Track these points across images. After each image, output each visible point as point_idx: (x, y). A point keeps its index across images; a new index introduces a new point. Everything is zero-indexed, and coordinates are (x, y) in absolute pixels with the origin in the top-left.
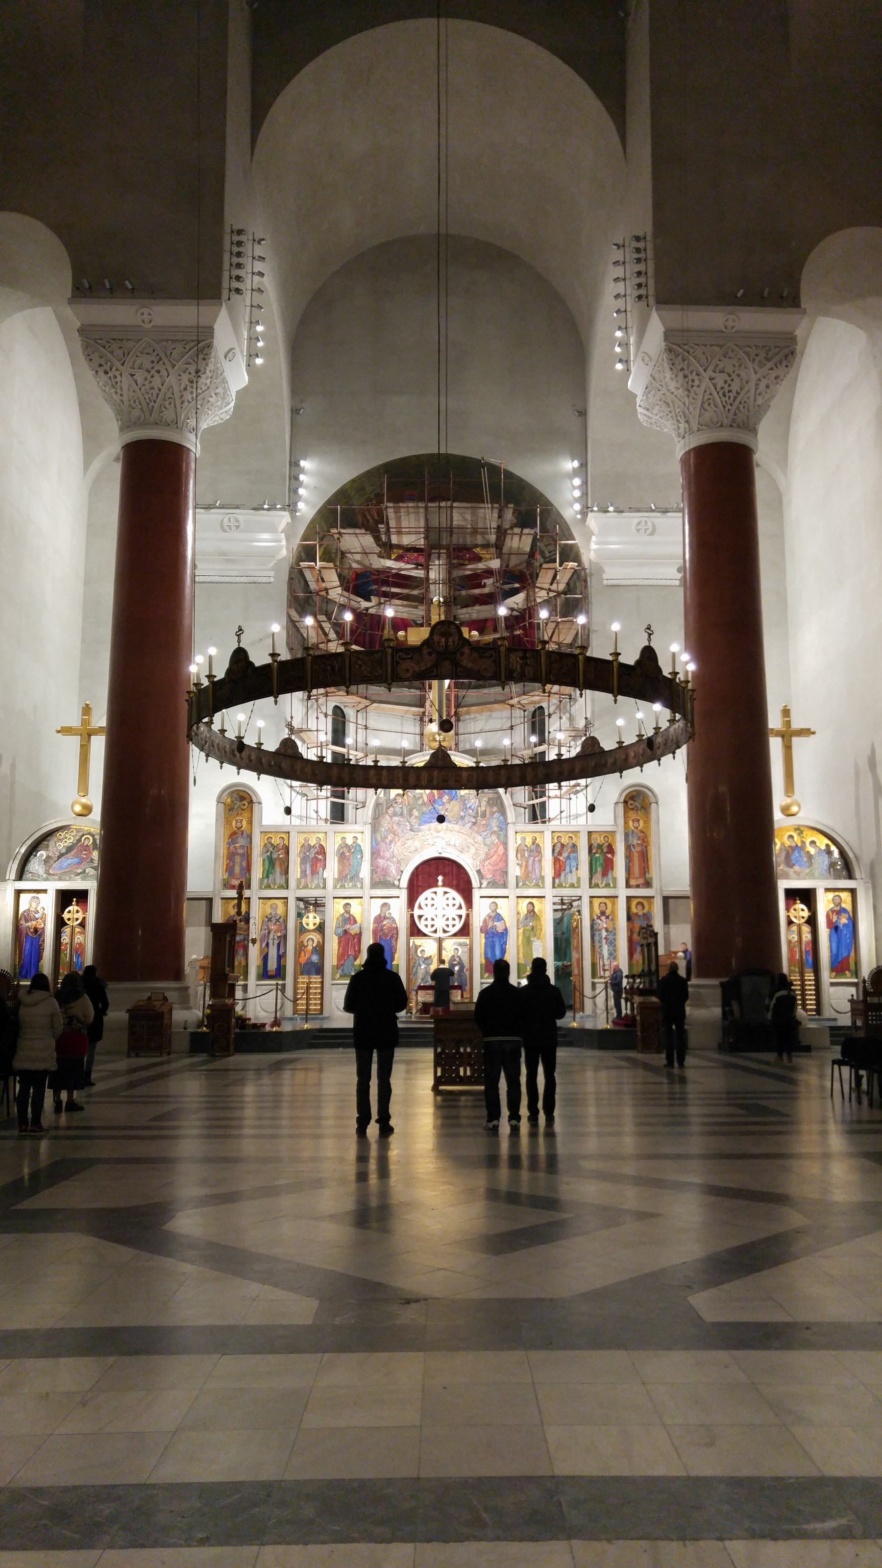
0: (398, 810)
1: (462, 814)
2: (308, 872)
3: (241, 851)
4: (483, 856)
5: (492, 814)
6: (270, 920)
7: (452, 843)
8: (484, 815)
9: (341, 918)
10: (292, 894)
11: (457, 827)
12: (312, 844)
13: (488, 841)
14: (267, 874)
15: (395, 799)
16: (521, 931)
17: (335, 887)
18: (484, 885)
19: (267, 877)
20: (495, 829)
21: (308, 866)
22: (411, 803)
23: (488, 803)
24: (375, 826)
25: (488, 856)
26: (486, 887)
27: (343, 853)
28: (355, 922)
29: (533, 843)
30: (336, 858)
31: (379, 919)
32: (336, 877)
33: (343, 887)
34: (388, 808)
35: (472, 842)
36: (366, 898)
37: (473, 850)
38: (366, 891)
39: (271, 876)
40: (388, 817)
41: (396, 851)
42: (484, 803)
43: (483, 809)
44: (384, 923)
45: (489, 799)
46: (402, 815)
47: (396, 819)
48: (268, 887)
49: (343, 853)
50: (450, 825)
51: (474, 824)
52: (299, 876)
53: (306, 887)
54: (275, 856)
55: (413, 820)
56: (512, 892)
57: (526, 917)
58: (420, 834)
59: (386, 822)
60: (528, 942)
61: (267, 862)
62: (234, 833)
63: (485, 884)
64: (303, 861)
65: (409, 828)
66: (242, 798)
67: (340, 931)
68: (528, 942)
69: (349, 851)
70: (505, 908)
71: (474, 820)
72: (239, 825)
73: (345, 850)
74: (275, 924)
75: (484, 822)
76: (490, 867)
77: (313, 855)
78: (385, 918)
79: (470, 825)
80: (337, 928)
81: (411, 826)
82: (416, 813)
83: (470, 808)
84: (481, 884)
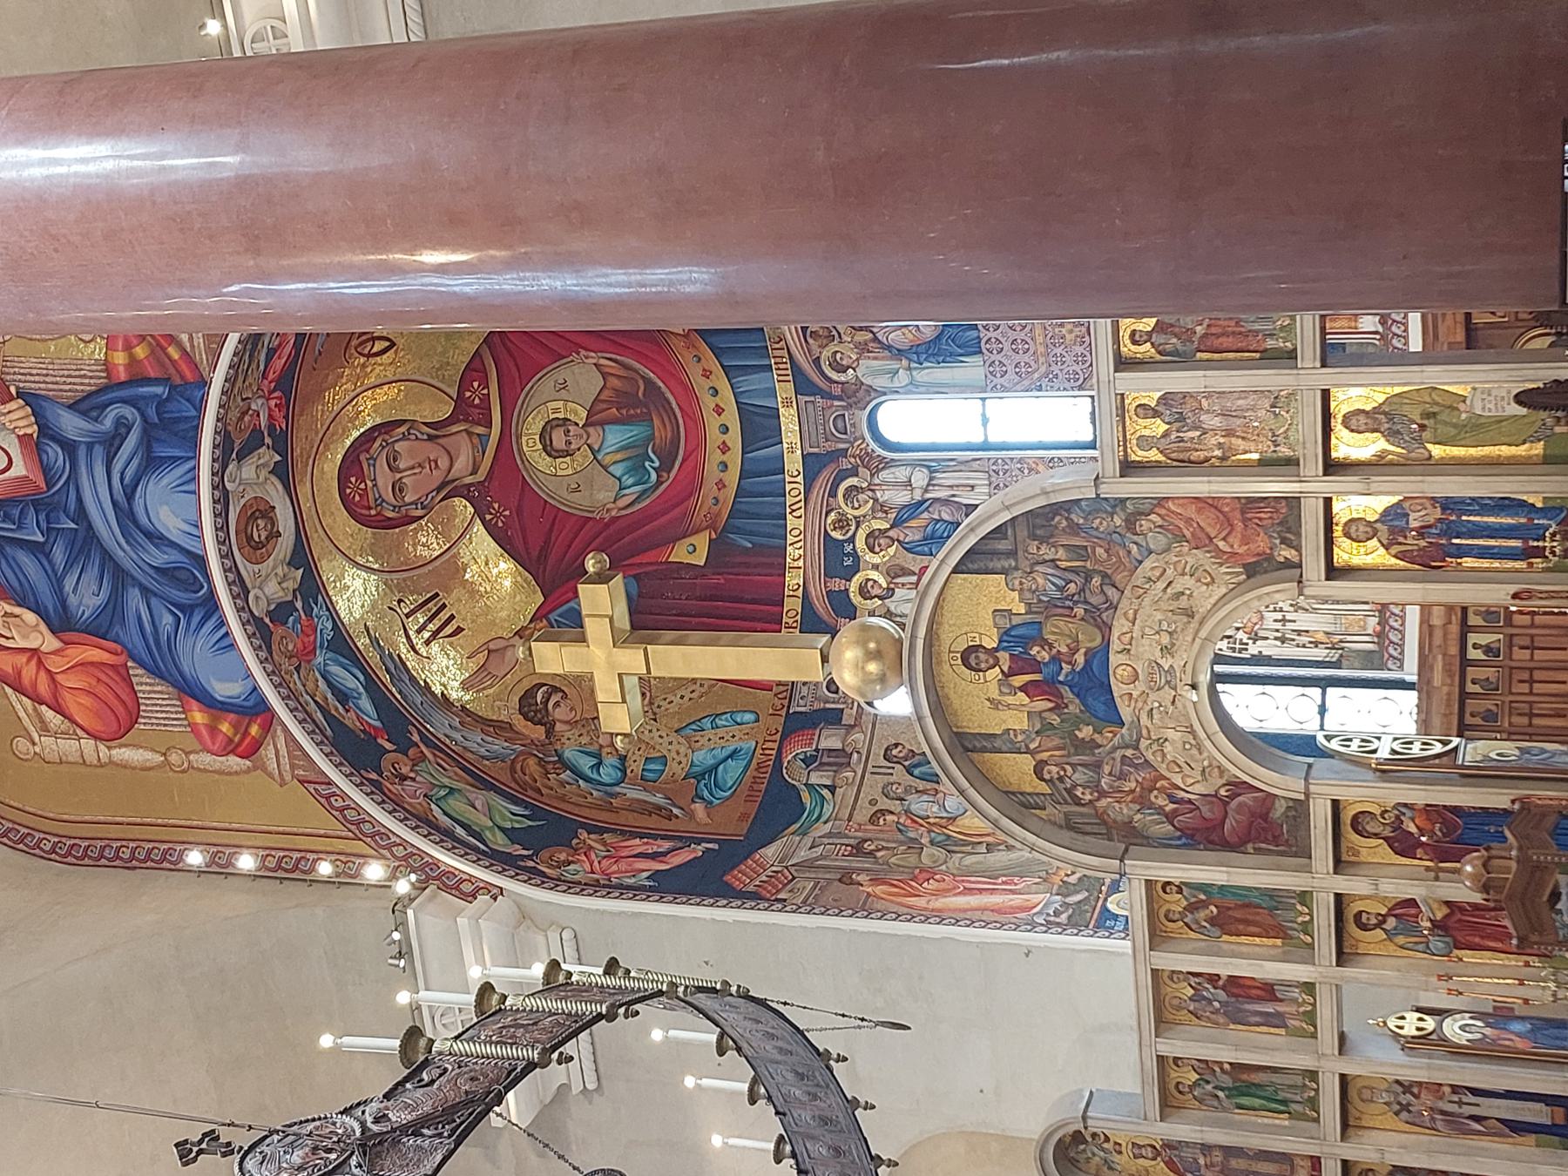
0: (1080, 776)
1: (1079, 611)
2: (1269, 1008)
3: (1218, 1157)
4: (1202, 557)
5: (1074, 529)
6: (1405, 1108)
7: (1165, 639)
8: (1080, 552)
9: (1401, 940)
10: (1331, 1069)
11: (1120, 626)
12: (1191, 992)
13: (1156, 541)
14: (1281, 1105)
15: (1049, 782)
16: (1437, 451)
17: (1306, 953)
18: (1288, 553)
19: (1284, 1102)
20: (1118, 521)
21: (1247, 1007)
22: (1057, 742)
23: (1042, 540)
24: (1130, 839)
25: (1202, 541)
26: (1298, 549)
27: (1212, 921)
28: (1412, 903)
29: (1156, 414)
30: (1225, 937)
31: (1403, 845)
32: (1279, 942)
33: (1307, 928)
34: (1077, 802)
35: (1161, 585)
36: (1343, 884)
37: (1186, 582)
38: (1316, 883)
39: (1281, 1095)
40: (1103, 802)
41: (1199, 789)
42: (1047, 552)
43: (1061, 553)
44: (1413, 829)
45: (1034, 537)
46: (1097, 766)
47: (1105, 783)
48: (1313, 1103)
49: (1212, 921)
50: (1115, 645)
51: (1105, 576)
52: (1282, 1031)
53: (1311, 1017)
54: (1227, 1081)
55: (1108, 738)
56: (1311, 486)
57: (1392, 435)
58: (1144, 720)
59: (1121, 810)
60: (1476, 430)
61: (1245, 1101)
62: (1170, 1164)
63: (1288, 553)
64: (1238, 1019)
65: (1129, 753)
66: (1077, 1137)
67: (1437, 943)
68: (1476, 430)
69: (1204, 904)
70: (1360, 503)
71: (1096, 581)
72: (1149, 1152)
73: (1202, 914)
74: (1417, 1097)
75: (1099, 551)
76: (1235, 540)
77: (1221, 994)
78: (1397, 824)
79: (1110, 591)
80: (1427, 950)
81: (1127, 747)
82: (1085, 732)
83: (1061, 589)
84: (1288, 564)
